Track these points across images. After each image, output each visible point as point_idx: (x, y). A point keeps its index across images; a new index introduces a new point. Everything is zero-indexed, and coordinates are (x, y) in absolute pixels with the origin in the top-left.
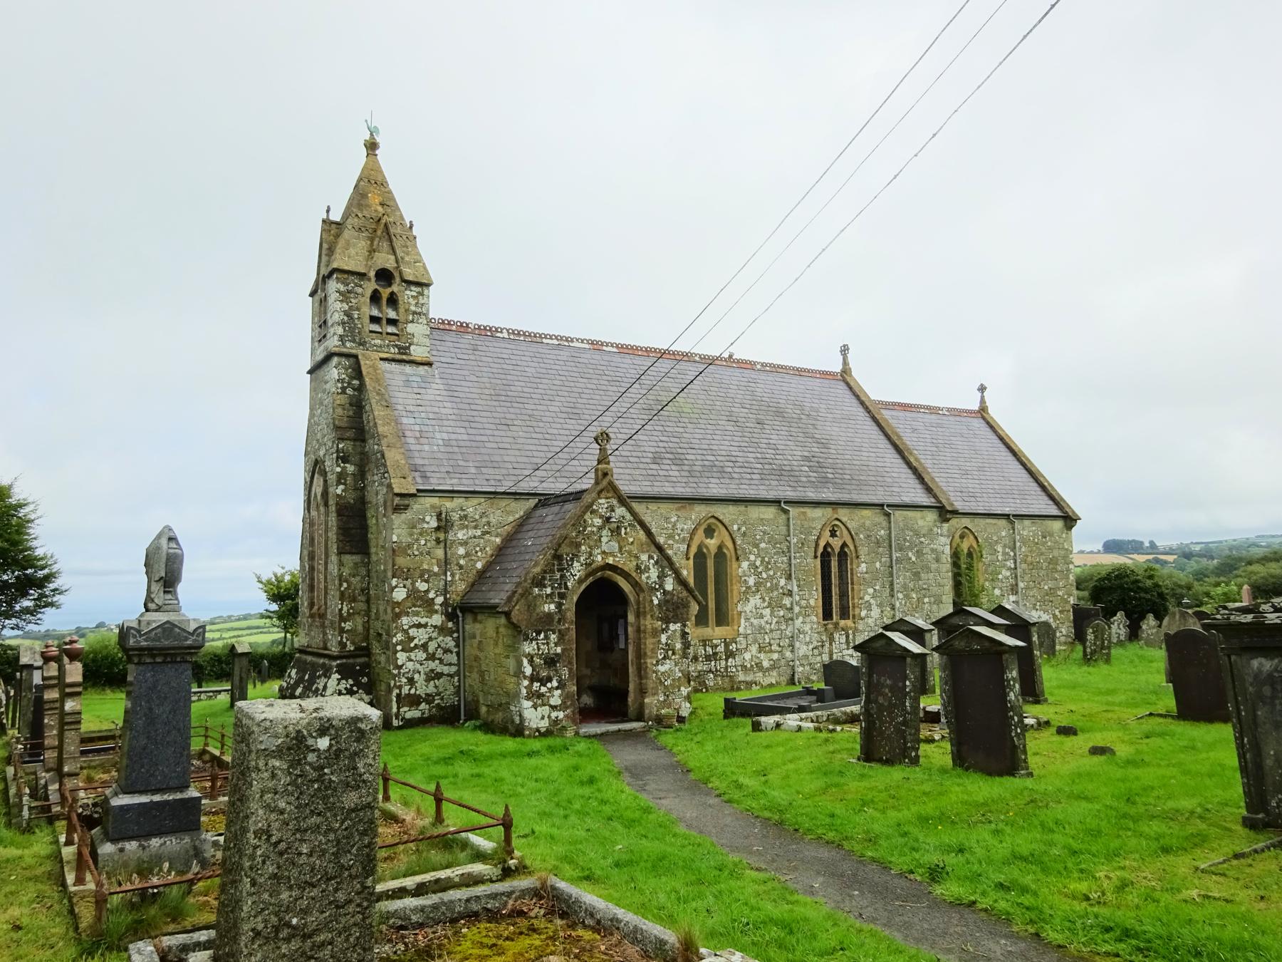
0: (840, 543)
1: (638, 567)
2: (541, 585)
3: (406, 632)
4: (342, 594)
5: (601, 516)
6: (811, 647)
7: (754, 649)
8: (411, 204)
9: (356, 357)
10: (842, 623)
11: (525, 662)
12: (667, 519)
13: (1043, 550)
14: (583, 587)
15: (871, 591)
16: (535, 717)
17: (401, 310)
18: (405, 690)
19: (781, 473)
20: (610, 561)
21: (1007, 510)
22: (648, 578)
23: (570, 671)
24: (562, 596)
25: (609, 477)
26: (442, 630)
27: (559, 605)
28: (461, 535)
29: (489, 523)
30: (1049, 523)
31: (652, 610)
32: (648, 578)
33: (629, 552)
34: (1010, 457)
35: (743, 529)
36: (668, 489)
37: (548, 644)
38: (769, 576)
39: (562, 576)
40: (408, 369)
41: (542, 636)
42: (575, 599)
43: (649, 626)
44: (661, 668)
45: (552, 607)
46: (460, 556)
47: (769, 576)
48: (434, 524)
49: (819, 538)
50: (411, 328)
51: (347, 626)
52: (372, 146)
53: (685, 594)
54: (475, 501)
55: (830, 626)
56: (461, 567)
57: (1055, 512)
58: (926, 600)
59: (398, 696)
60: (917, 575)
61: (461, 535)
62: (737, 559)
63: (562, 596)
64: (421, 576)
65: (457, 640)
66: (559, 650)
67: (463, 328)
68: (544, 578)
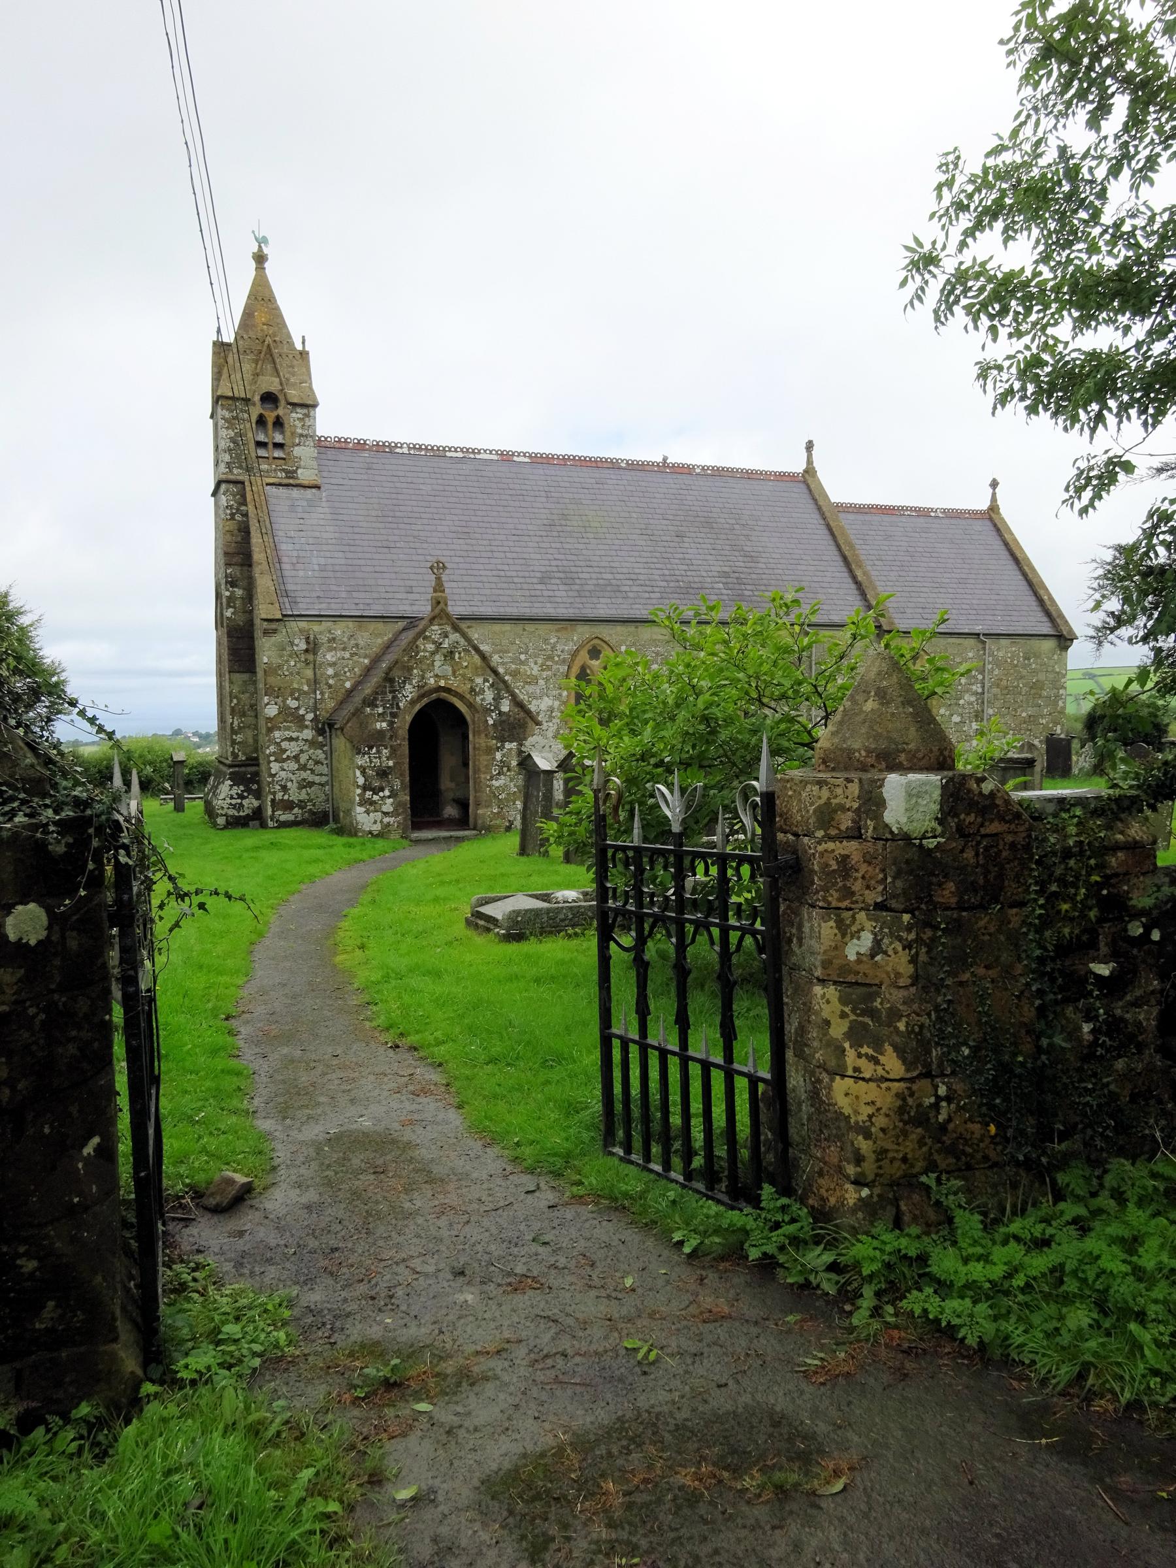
1: (472, 690)
2: (373, 705)
3: (278, 744)
4: (233, 709)
5: (434, 642)
8: (300, 322)
9: (243, 483)
11: (358, 773)
12: (546, 641)
13: (1024, 672)
14: (418, 707)
16: (365, 819)
17: (288, 434)
18: (279, 796)
20: (442, 683)
21: (978, 629)
24: (394, 715)
25: (442, 605)
26: (312, 743)
27: (391, 724)
28: (329, 657)
29: (357, 645)
30: (1035, 643)
33: (463, 676)
34: (1011, 565)
36: (550, 610)
40: (295, 493)
42: (409, 719)
45: (384, 725)
48: (303, 646)
50: (297, 451)
51: (239, 738)
52: (260, 259)
53: (522, 715)
54: (343, 624)
56: (330, 686)
57: (1046, 628)
59: (273, 801)
61: (329, 657)
63: (394, 715)
64: (292, 695)
67: (361, 445)
68: (375, 699)
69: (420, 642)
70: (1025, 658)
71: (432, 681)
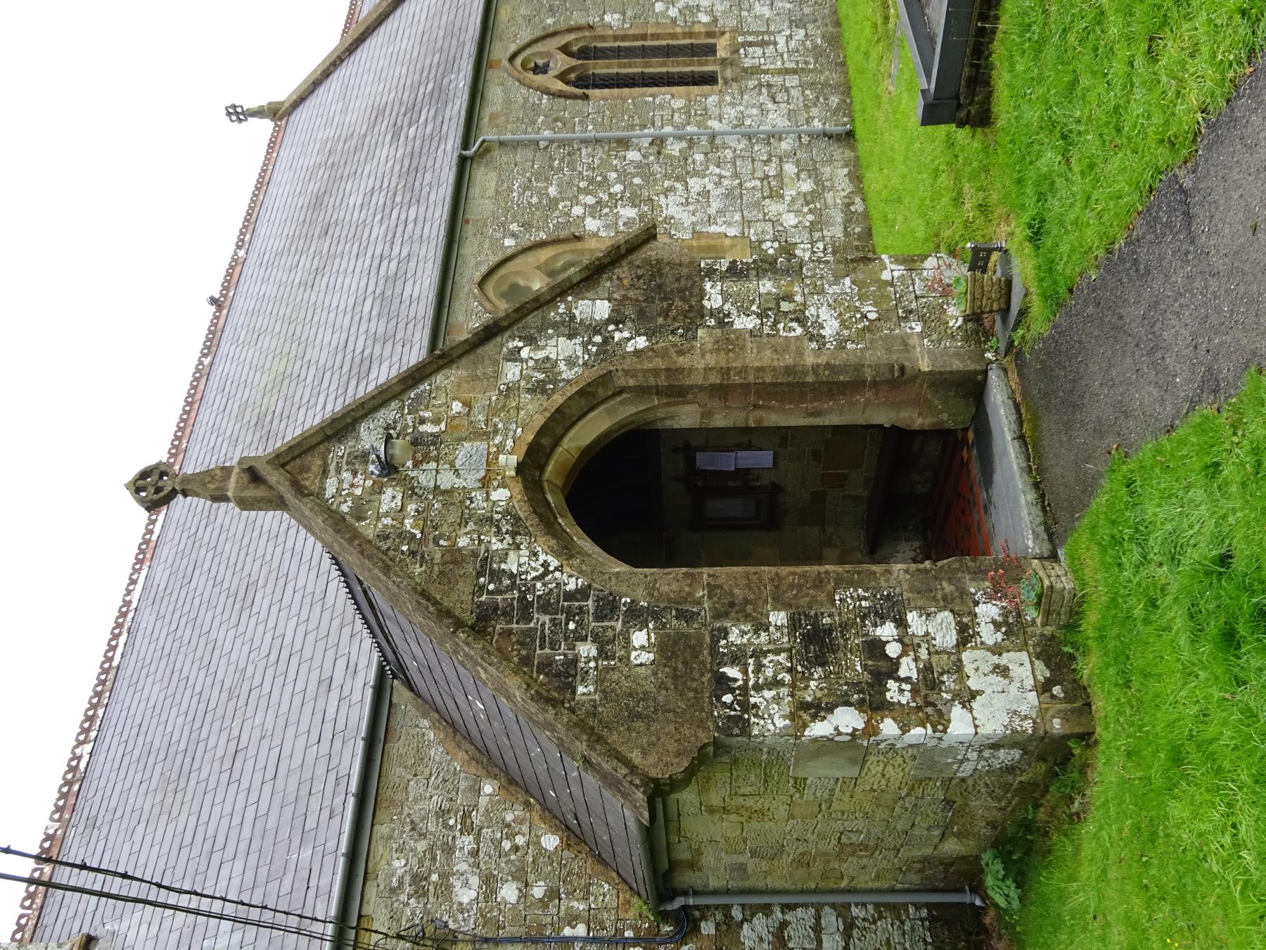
0: (561, 57)
1: (539, 389)
2: (568, 673)
5: (378, 489)
6: (770, 106)
7: (773, 208)
10: (721, 53)
11: (819, 729)
14: (587, 544)
16: (1000, 701)
19: (413, 170)
20: (509, 462)
22: (571, 362)
23: (840, 582)
24: (608, 607)
27: (636, 616)
29: (442, 813)
31: (664, 353)
32: (571, 362)
33: (491, 411)
35: (514, 227)
37: (759, 654)
38: (618, 180)
39: (546, 606)
41: (732, 672)
42: (620, 568)
43: (711, 360)
44: (831, 328)
45: (639, 638)
46: (524, 895)
47: (618, 180)
49: (546, 91)
53: (623, 271)
55: (729, 73)
56: (553, 894)
61: (465, 896)
62: (578, 238)
63: (608, 607)
65: (751, 912)
66: (778, 618)
69: (368, 529)
71: (500, 495)
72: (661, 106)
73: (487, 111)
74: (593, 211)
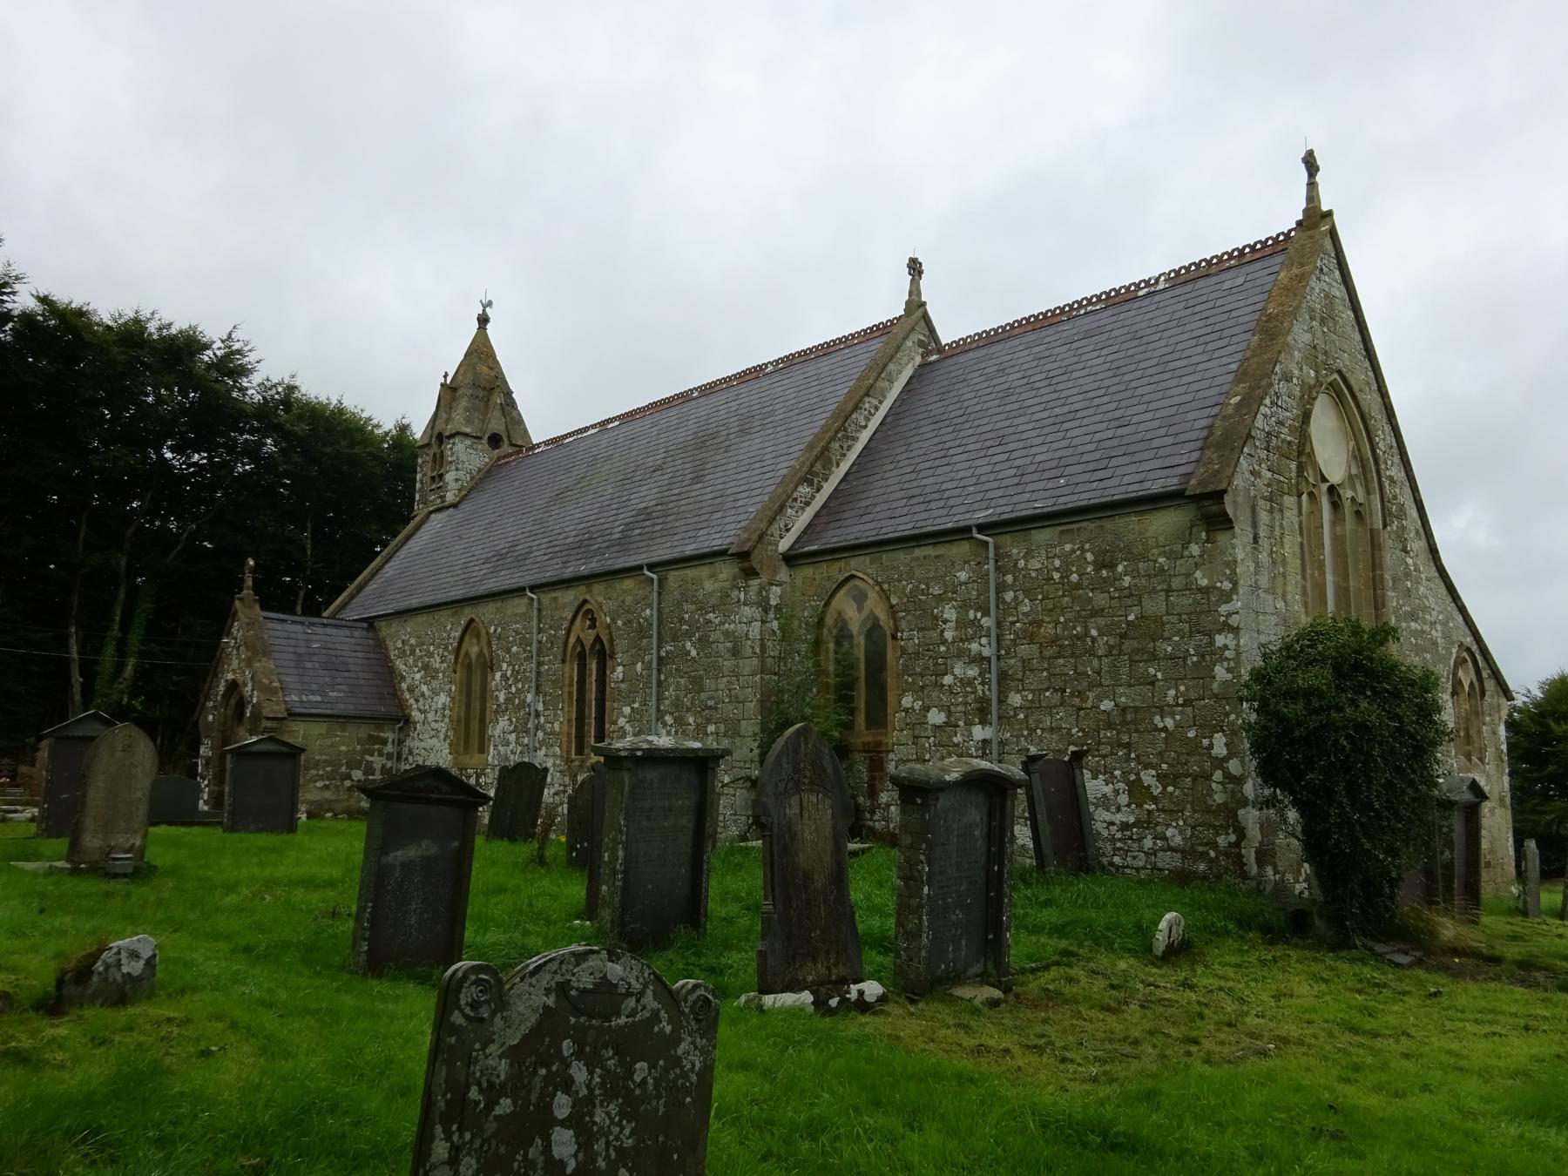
13: (1101, 600)
15: (627, 710)
58: (711, 728)
60: (697, 684)
70: (1099, 566)
72: (555, 715)
73: (557, 594)
74: (504, 676)
